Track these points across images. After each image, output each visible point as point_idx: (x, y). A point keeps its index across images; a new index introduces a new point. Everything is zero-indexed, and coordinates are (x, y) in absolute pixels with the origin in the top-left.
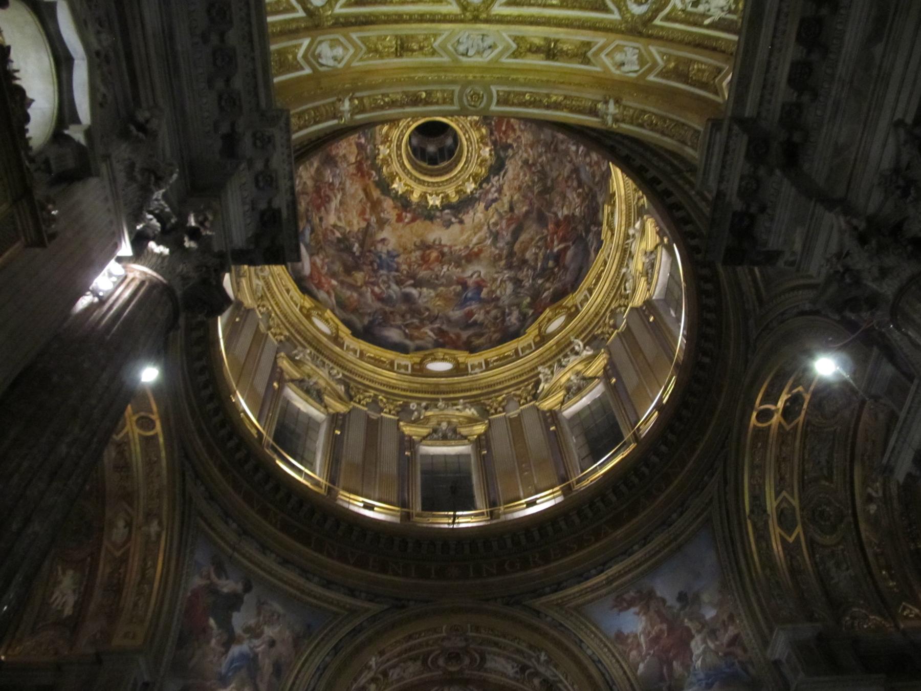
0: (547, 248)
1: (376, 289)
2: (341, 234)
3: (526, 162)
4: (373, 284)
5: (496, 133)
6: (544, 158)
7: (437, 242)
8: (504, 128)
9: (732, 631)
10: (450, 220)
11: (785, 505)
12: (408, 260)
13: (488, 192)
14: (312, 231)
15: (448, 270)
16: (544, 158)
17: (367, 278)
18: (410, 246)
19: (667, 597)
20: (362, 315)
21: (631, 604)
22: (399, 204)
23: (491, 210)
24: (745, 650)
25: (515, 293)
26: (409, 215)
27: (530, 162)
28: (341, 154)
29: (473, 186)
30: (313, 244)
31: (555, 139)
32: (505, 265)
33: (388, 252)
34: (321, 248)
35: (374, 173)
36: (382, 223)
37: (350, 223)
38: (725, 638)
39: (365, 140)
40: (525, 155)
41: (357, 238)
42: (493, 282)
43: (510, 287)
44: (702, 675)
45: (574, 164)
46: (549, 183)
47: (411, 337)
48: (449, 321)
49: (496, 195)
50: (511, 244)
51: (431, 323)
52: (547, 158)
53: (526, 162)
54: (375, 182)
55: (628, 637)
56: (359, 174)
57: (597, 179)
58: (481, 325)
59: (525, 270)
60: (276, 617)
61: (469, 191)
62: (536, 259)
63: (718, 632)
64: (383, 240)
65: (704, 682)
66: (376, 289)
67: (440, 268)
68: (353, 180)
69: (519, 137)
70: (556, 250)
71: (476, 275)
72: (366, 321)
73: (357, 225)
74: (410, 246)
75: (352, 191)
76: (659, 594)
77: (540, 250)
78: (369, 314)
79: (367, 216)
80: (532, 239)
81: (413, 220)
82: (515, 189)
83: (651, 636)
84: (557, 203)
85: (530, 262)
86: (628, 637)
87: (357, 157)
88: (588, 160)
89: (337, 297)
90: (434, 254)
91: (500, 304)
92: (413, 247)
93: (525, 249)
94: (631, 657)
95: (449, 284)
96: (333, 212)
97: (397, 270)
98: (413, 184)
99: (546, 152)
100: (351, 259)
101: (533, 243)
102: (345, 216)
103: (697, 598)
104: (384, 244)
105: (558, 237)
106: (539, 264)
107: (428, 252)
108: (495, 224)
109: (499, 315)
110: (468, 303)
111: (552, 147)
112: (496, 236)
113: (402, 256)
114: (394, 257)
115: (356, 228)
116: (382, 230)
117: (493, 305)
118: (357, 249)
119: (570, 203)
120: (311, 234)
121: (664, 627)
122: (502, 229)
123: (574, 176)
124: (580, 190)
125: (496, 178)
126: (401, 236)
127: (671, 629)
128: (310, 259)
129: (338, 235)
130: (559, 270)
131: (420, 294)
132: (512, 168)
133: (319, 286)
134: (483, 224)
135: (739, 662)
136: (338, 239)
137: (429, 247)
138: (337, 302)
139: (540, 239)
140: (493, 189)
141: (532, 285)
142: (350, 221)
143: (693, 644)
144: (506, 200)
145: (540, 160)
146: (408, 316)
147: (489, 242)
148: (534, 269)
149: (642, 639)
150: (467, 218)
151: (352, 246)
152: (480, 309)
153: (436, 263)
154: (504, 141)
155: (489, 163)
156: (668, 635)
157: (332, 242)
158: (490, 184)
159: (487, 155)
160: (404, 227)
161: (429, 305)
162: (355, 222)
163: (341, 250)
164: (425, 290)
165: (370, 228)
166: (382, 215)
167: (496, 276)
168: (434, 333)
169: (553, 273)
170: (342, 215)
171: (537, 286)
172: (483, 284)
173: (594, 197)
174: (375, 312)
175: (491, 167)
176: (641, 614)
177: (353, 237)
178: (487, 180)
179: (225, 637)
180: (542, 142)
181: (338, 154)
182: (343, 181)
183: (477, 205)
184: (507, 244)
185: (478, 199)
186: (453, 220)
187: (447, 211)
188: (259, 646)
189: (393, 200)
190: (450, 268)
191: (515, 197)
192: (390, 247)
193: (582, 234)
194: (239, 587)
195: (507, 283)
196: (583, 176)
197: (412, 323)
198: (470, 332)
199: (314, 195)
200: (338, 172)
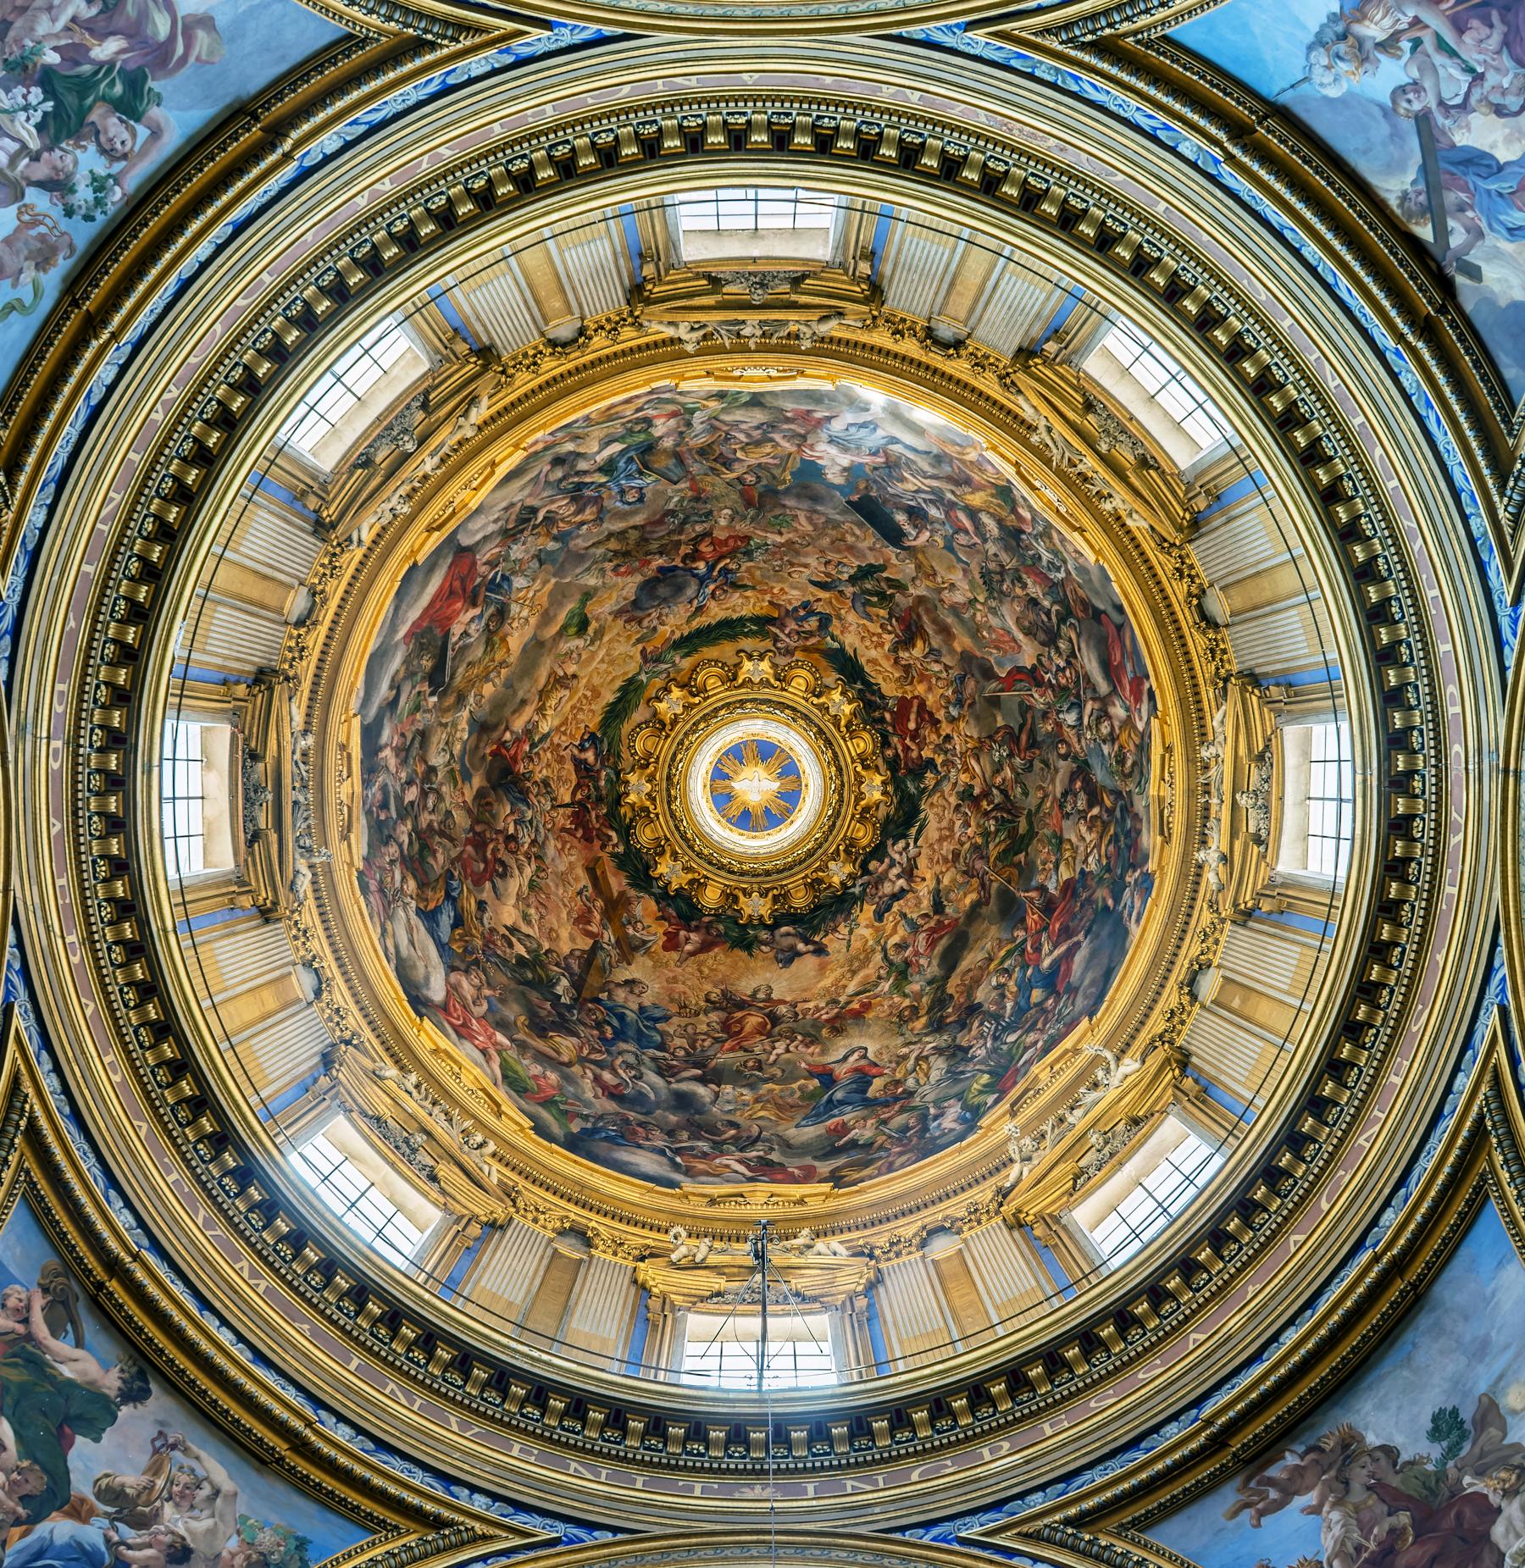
0: (1024, 967)
1: (607, 1076)
2: (528, 952)
3: (967, 795)
4: (600, 1064)
5: (895, 739)
6: (1008, 773)
7: (761, 996)
8: (912, 725)
10: (792, 948)
12: (690, 1029)
13: (882, 878)
14: (458, 922)
15: (788, 1051)
16: (1008, 773)
17: (585, 1052)
18: (696, 1000)
19: (1398, 1440)
20: (568, 1115)
21: (1288, 1494)
22: (671, 911)
23: (889, 918)
25: (953, 1075)
26: (693, 936)
27: (977, 791)
28: (538, 777)
29: (849, 868)
30: (457, 948)
31: (1029, 716)
32: (926, 1026)
33: (642, 1009)
34: (477, 962)
35: (613, 834)
36: (629, 949)
37: (552, 935)
39: (597, 755)
40: (964, 778)
41: (568, 968)
42: (898, 1064)
43: (939, 1066)
45: (1075, 758)
46: (1023, 826)
47: (689, 1172)
48: (787, 1146)
49: (901, 882)
50: (939, 983)
51: (741, 1150)
52: (1013, 769)
53: (967, 795)
54: (614, 855)
56: (579, 834)
57: (1129, 763)
58: (869, 1145)
59: (976, 1024)
60: (207, 1490)
61: (836, 880)
62: (1003, 996)
64: (630, 983)
66: (607, 1076)
67: (768, 1048)
68: (564, 843)
69: (948, 738)
70: (1046, 963)
71: (856, 1056)
72: (575, 1127)
73: (568, 941)
74: (696, 1000)
75: (562, 868)
77: (1010, 977)
78: (586, 1118)
79: (594, 929)
80: (990, 959)
81: (705, 947)
82: (946, 860)
83: (1365, 1555)
84: (1044, 863)
85: (986, 1006)
87: (574, 794)
88: (1105, 729)
89: (504, 1066)
90: (753, 1020)
91: (917, 1101)
92: (702, 1003)
93: (977, 982)
95: (789, 1075)
96: (512, 901)
97: (662, 1047)
98: (704, 870)
99: (1011, 755)
100: (548, 1005)
101: (992, 967)
102: (542, 917)
103: (1490, 1412)
104: (632, 992)
105: (1049, 937)
106: (1009, 1005)
107: (739, 1015)
108: (900, 947)
109: (912, 1122)
110: (836, 1111)
111: (1024, 737)
112: (902, 973)
113: (675, 1020)
114: (657, 1020)
115: (565, 947)
116: (629, 964)
117: (897, 1107)
118: (566, 990)
119: (1075, 849)
120: (454, 926)
121: (1404, 1518)
122: (917, 954)
123: (1079, 784)
124: (1095, 811)
125: (901, 844)
126: (675, 980)
128: (447, 975)
129: (522, 951)
130: (1056, 1003)
131: (717, 1095)
132: (937, 815)
133: (463, 1032)
134: (873, 951)
136: (520, 958)
137: (742, 1005)
138: (505, 1077)
139: (1009, 954)
140: (896, 871)
141: (995, 1050)
142: (551, 929)
143: (1498, 1531)
144: (924, 890)
145: (999, 780)
146: (685, 1135)
147: (886, 986)
148: (997, 1017)
150: (834, 943)
151: (552, 983)
152: (865, 1119)
153: (759, 1038)
154: (914, 755)
155: (882, 812)
156: (1416, 1537)
157: (505, 961)
158: (887, 860)
159: (877, 796)
160: (681, 961)
161: (737, 1118)
162: (564, 933)
163: (527, 983)
164: (728, 1089)
165: (601, 955)
166: (631, 931)
167: (905, 1050)
168: (748, 1167)
169: (1044, 1011)
170: (532, 911)
171: (1005, 1047)
172: (874, 1071)
173: (1127, 809)
174: (601, 1117)
175: (888, 820)
176: (1326, 1508)
177: (557, 965)
178: (879, 852)
179: (36, 1483)
180: (999, 737)
181: (527, 777)
182: (540, 840)
183: (856, 911)
184: (929, 983)
185: (861, 898)
186: (801, 946)
187: (784, 929)
188: (140, 1547)
189: (658, 903)
190: (791, 1048)
191: (946, 881)
192: (647, 1000)
193: (1106, 908)
194: (111, 1382)
195: (932, 1059)
196: (1099, 775)
197: (692, 1148)
198: (841, 1161)
199: (469, 848)
200: (529, 814)
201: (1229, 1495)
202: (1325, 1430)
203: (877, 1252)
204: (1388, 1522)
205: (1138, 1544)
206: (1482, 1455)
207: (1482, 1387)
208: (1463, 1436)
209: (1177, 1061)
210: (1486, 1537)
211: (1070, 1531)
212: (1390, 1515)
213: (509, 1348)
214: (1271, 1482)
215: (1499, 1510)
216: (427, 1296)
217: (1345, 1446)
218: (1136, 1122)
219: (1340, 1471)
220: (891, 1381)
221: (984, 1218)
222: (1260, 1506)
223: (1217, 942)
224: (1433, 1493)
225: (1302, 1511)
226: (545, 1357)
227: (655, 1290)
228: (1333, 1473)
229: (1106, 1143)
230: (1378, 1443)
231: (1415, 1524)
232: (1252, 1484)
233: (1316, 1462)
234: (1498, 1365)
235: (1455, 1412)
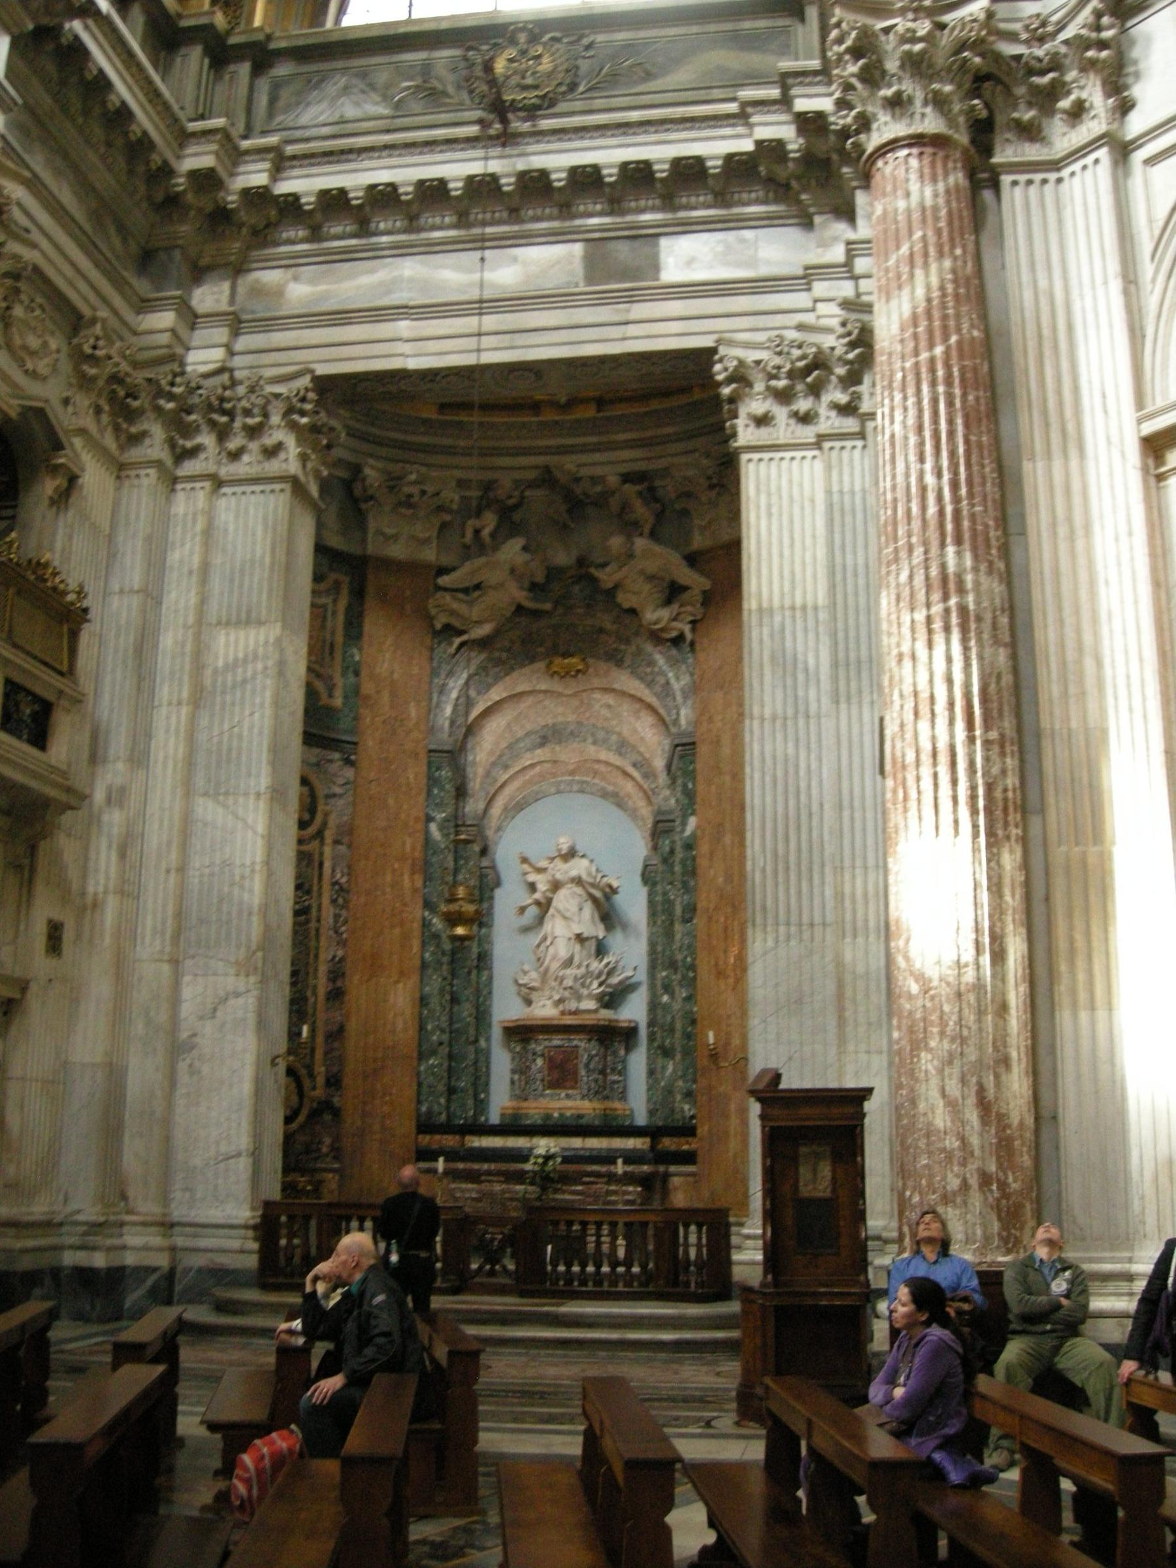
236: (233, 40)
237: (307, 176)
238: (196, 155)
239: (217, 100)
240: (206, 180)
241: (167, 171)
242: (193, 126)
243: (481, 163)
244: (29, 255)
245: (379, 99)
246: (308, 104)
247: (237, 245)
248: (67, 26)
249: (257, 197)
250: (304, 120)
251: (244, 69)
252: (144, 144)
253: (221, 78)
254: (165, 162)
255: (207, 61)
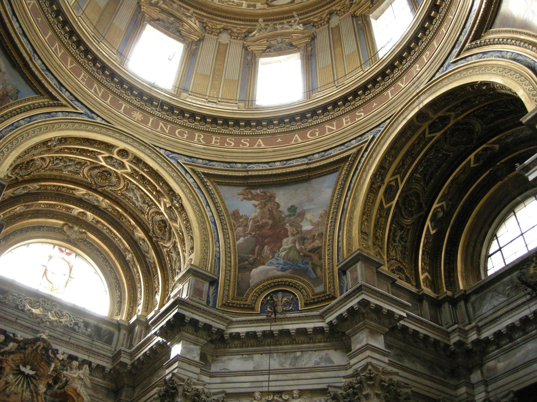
9: (317, 243)
11: (393, 183)
19: (282, 204)
21: (253, 198)
24: (320, 258)
38: (309, 247)
44: (281, 261)
55: (241, 217)
63: (306, 241)
65: (281, 266)
76: (277, 200)
83: (258, 224)
86: (241, 217)
94: (237, 230)
103: (302, 215)
121: (270, 222)
127: (273, 226)
135: (312, 264)
143: (285, 240)
149: (250, 223)
156: (270, 228)
176: (258, 207)
201: (241, 190)
202: (269, 191)
203: (207, 28)
204: (267, 220)
205: (214, 187)
206: (294, 222)
207: (305, 208)
208: (294, 215)
209: (312, 37)
210: (282, 239)
211: (203, 176)
212: (269, 219)
213: (92, 43)
214: (251, 194)
215: (288, 236)
216: (77, 20)
217: (271, 197)
218: (291, 45)
219: (266, 201)
220: (185, 102)
221: (239, 38)
222: (246, 197)
223: (344, 12)
224: (280, 222)
225: (253, 204)
226: (101, 50)
227: (142, 10)
228: (264, 201)
229: (281, 43)
230: (278, 202)
231: (272, 225)
232: (247, 191)
233: (263, 196)
234: (311, 207)
235: (296, 208)
236: (456, 296)
237: (488, 330)
238: (454, 337)
239: (458, 315)
240: (459, 344)
241: (447, 346)
242: (450, 330)
243: (528, 309)
244: (409, 391)
245: (502, 296)
246: (483, 306)
247: (477, 358)
248: (398, 324)
249: (477, 342)
250: (484, 311)
251: (462, 303)
252: (436, 342)
253: (457, 308)
254: (445, 344)
255: (450, 306)
